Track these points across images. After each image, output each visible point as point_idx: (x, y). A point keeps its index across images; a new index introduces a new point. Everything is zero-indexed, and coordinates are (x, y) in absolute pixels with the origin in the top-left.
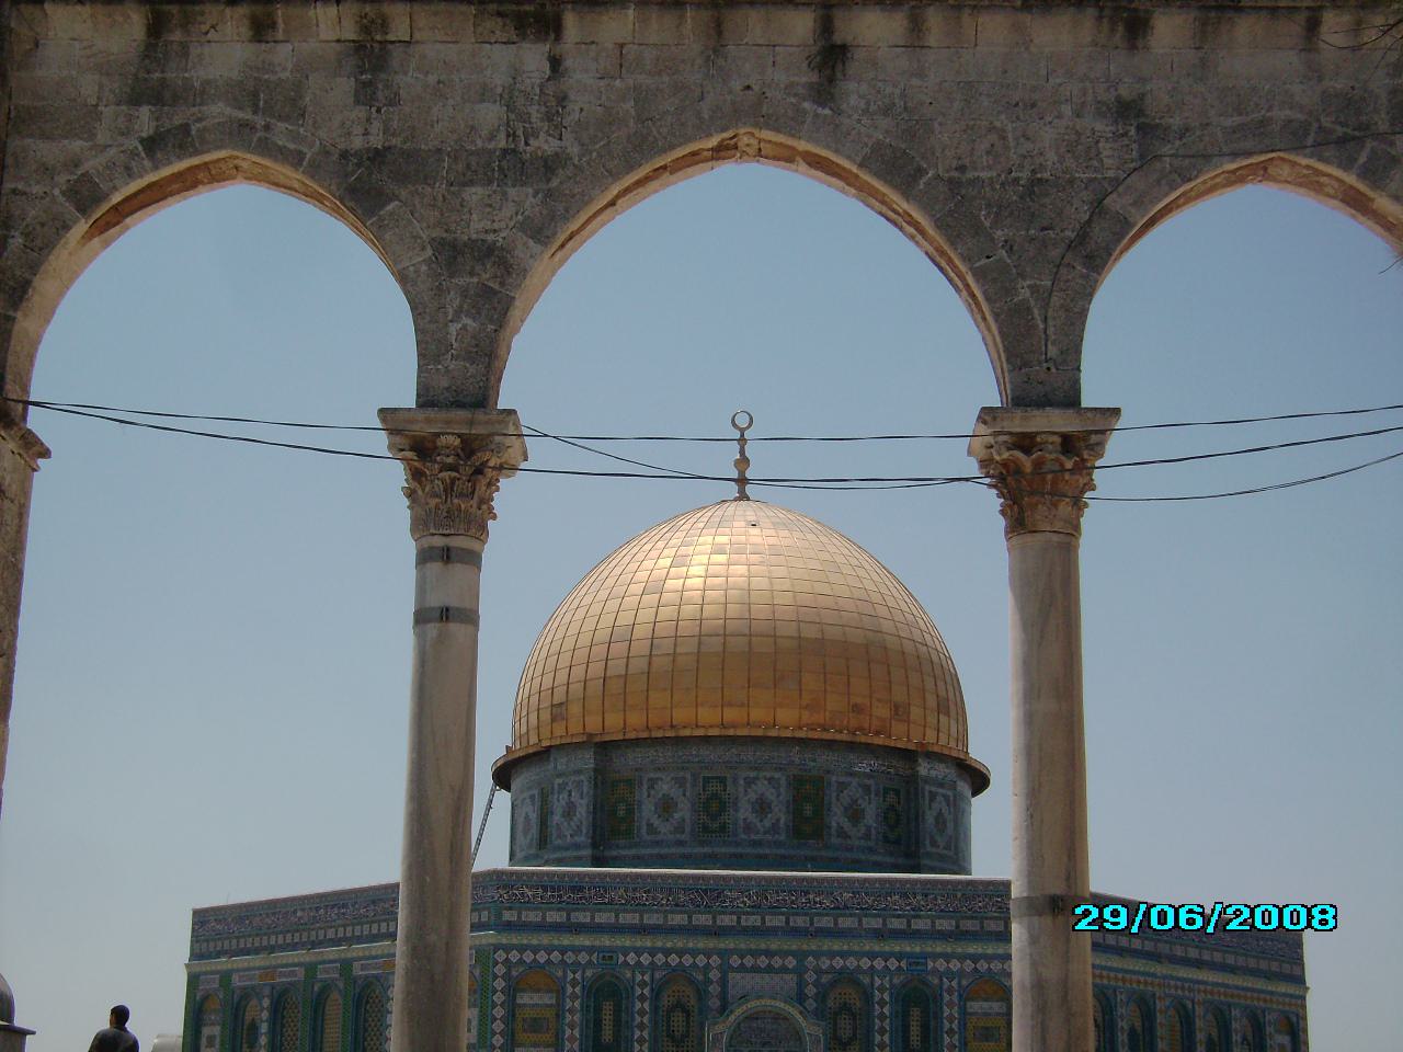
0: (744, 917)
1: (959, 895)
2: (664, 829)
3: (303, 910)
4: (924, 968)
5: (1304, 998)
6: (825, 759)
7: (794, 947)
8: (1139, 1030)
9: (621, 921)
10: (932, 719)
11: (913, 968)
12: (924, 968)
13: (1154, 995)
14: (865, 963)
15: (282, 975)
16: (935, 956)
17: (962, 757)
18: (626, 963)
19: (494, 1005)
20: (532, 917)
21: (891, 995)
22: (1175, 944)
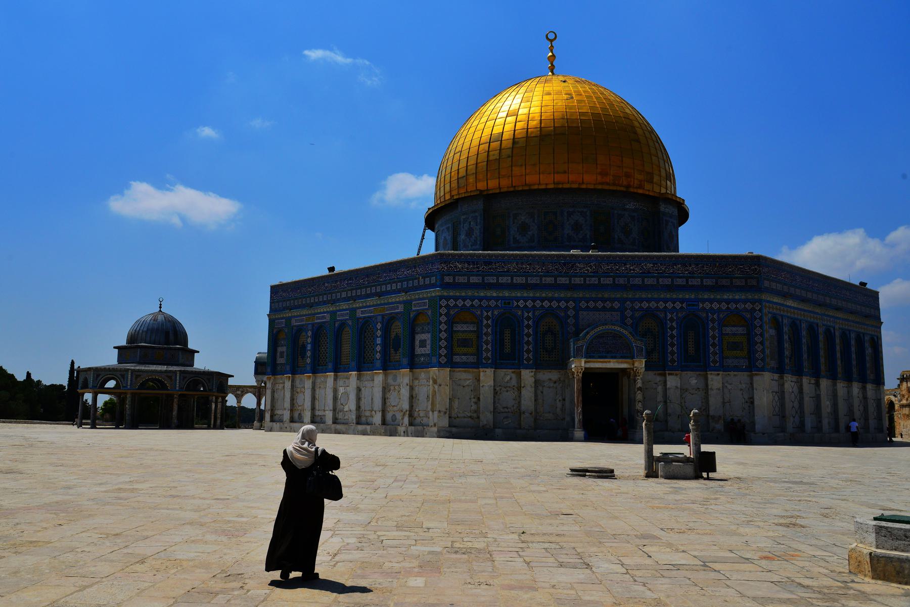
3: (328, 283)
7: (618, 296)
9: (515, 281)
10: (663, 183)
13: (817, 325)
14: (661, 305)
16: (704, 301)
17: (681, 202)
18: (518, 306)
19: (441, 331)
20: (462, 280)
21: (677, 323)
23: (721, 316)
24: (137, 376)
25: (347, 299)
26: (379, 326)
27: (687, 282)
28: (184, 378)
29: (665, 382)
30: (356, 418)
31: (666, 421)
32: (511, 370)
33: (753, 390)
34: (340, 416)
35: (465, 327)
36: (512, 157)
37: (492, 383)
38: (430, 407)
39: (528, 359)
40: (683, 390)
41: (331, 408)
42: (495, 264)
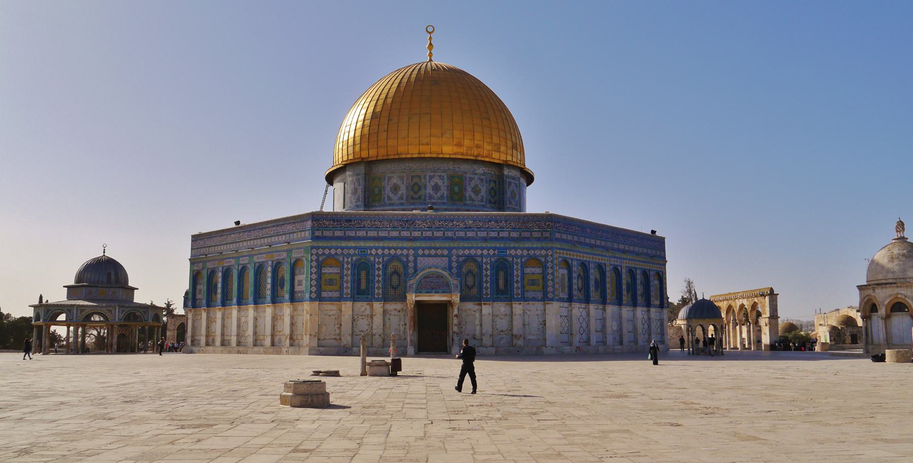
2: (395, 199)
4: (505, 254)
5: (665, 265)
6: (465, 167)
9: (369, 235)
14: (479, 252)
17: (522, 167)
18: (371, 254)
20: (328, 234)
22: (614, 242)
23: (523, 260)
24: (82, 311)
26: (270, 269)
27: (499, 235)
28: (123, 311)
29: (481, 310)
30: (253, 341)
31: (482, 340)
32: (366, 303)
33: (545, 314)
34: (242, 340)
35: (331, 270)
36: (387, 131)
38: (304, 332)
39: (378, 294)
40: (494, 316)
42: (354, 221)
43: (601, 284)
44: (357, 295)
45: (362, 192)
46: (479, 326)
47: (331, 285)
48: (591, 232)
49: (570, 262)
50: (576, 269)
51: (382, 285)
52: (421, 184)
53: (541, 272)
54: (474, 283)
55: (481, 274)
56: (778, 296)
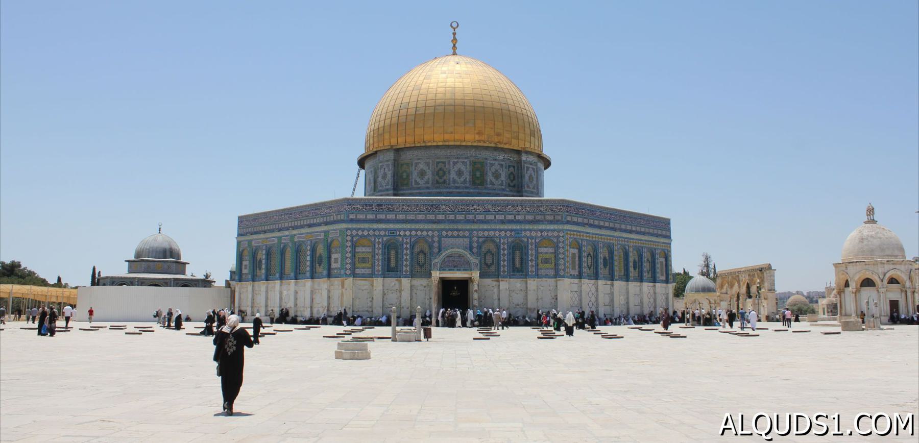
0: (448, 216)
1: (535, 205)
2: (421, 182)
3: (276, 216)
4: (520, 235)
5: (670, 244)
6: (486, 154)
7: (468, 227)
8: (607, 258)
9: (398, 218)
10: (528, 138)
11: (517, 235)
12: (520, 235)
13: (613, 243)
14: (497, 233)
15: (270, 241)
16: (526, 230)
17: (540, 153)
18: (400, 235)
19: (347, 252)
25: (288, 229)
26: (309, 248)
29: (499, 286)
35: (364, 250)
37: (381, 288)
39: (406, 271)
41: (278, 305)
43: (609, 262)
44: (387, 272)
45: (391, 177)
46: (497, 300)
47: (363, 263)
48: (600, 215)
49: (581, 242)
50: (587, 249)
51: (410, 263)
52: (445, 170)
53: (553, 251)
54: (493, 261)
55: (499, 253)
56: (775, 272)
